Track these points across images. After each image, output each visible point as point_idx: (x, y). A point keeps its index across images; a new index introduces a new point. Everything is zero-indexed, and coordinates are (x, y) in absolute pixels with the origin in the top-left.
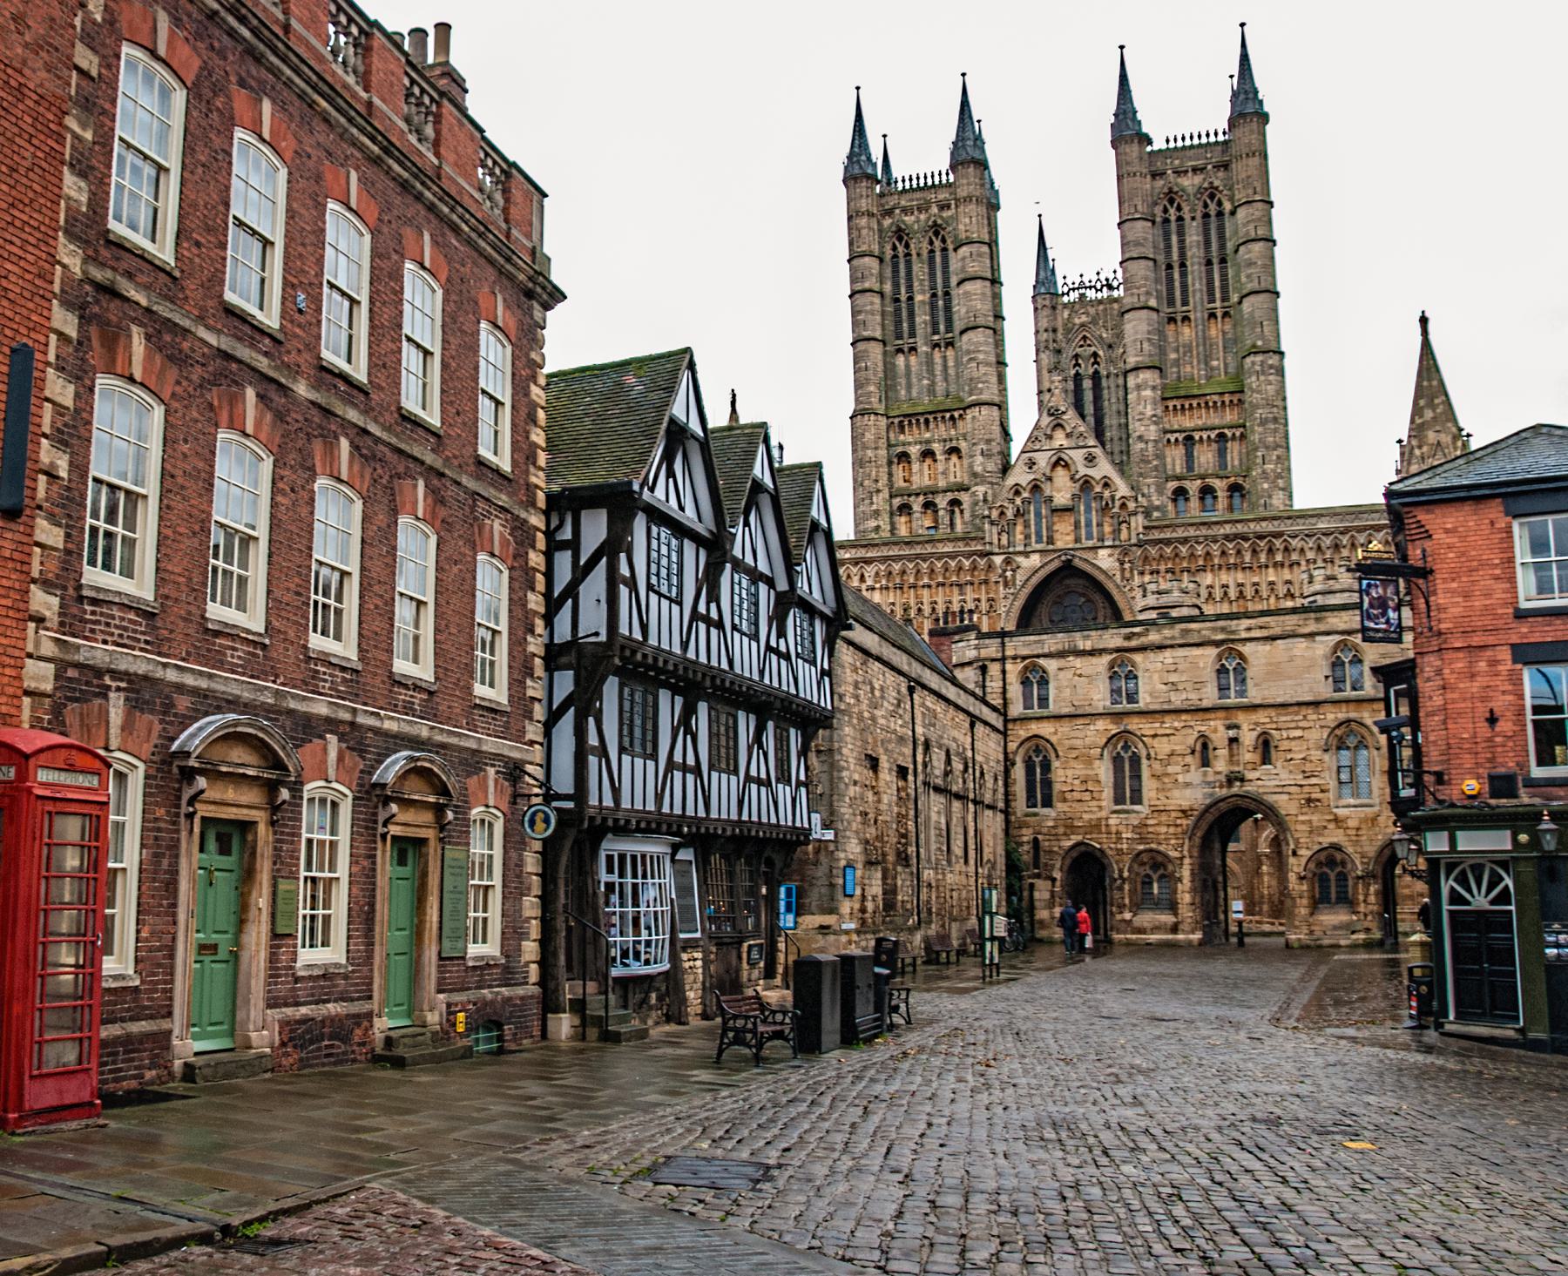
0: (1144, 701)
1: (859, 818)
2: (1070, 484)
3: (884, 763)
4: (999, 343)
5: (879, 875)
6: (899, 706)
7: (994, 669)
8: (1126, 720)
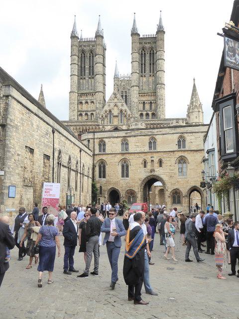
0: (131, 150)
1: (20, 169)
3: (36, 151)
4: (104, 79)
5: (32, 191)
6: (47, 134)
7: (91, 141)
8: (125, 155)
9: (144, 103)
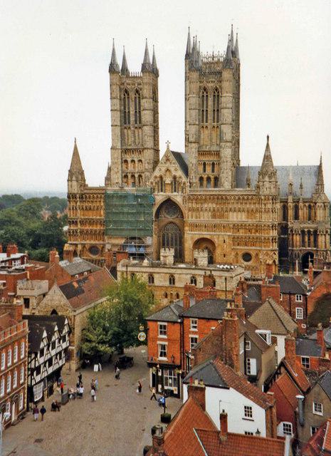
9: (205, 164)
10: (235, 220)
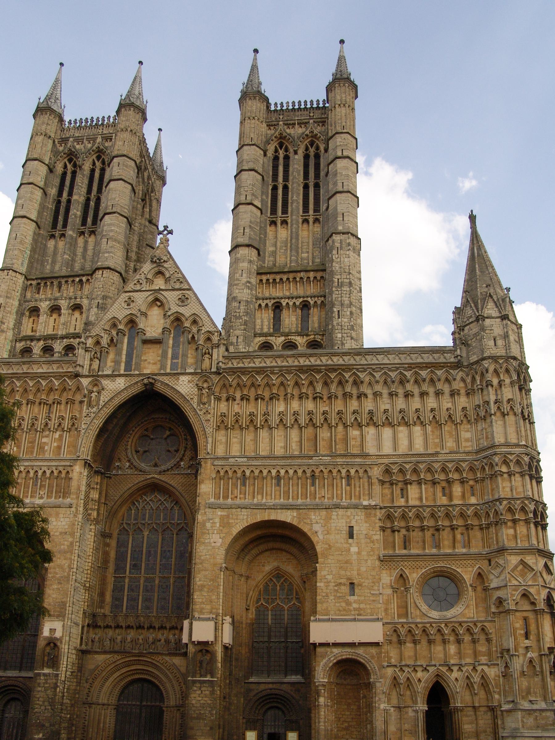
2: (162, 321)
10: (387, 449)
